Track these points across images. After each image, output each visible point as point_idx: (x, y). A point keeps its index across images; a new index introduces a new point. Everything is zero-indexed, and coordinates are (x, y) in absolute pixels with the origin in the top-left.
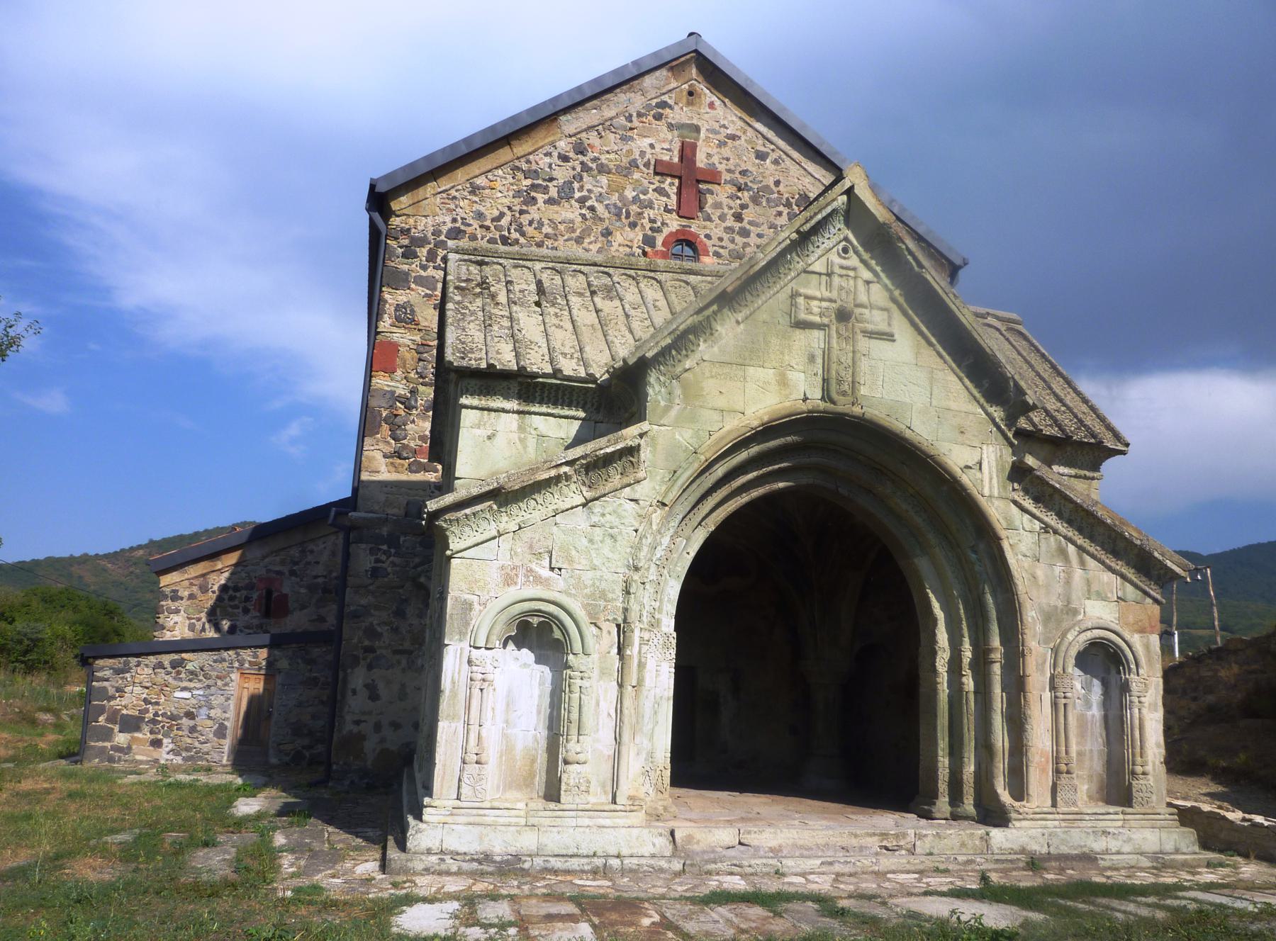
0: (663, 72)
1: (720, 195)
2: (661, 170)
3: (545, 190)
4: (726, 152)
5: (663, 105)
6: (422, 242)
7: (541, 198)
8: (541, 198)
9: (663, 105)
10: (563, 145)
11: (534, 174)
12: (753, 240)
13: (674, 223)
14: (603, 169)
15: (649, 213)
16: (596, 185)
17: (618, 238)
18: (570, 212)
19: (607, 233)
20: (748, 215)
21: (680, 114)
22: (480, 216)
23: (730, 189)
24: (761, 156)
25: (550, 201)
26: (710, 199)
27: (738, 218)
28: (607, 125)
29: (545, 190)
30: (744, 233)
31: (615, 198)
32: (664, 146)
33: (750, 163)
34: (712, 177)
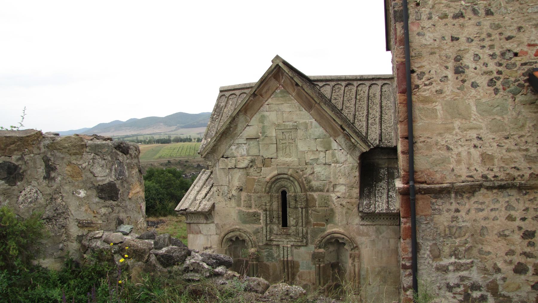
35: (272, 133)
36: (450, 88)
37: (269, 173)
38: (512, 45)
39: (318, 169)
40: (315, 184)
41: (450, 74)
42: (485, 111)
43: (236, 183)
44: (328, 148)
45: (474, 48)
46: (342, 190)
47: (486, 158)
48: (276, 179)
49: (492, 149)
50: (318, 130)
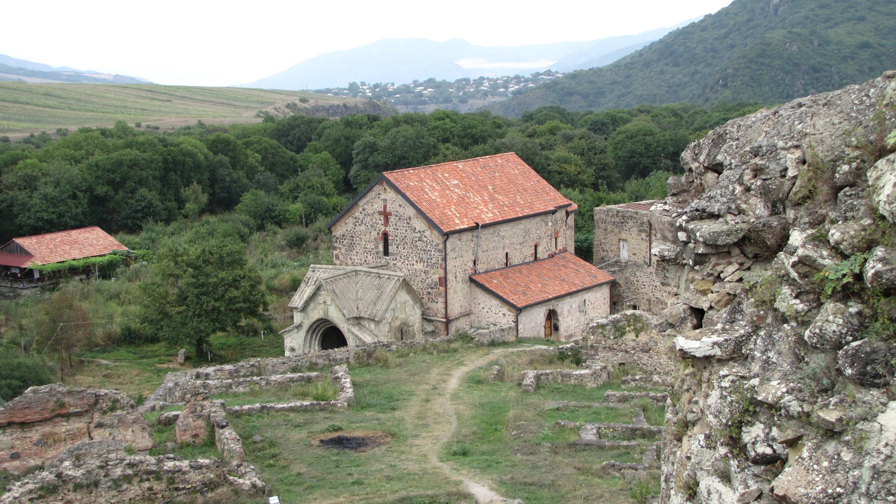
0: (377, 186)
1: (392, 219)
2: (380, 213)
3: (358, 222)
4: (393, 206)
5: (379, 194)
6: (337, 238)
7: (357, 224)
8: (357, 224)
9: (379, 194)
10: (361, 209)
11: (356, 218)
12: (399, 231)
13: (383, 229)
14: (369, 215)
15: (378, 226)
16: (368, 219)
17: (373, 234)
18: (363, 228)
19: (370, 233)
20: (398, 224)
21: (383, 196)
22: (347, 230)
23: (394, 217)
24: (400, 206)
25: (360, 225)
26: (390, 220)
27: (396, 225)
28: (368, 202)
29: (358, 222)
30: (397, 229)
31: (371, 223)
32: (378, 206)
33: (398, 208)
34: (390, 214)
35: (399, 306)
36: (454, 284)
37: (398, 323)
38: (466, 267)
39: (411, 318)
40: (410, 324)
41: (454, 279)
42: (461, 291)
43: (387, 330)
44: (414, 308)
45: (459, 270)
46: (417, 324)
47: (461, 306)
48: (400, 324)
49: (462, 303)
50: (411, 302)
